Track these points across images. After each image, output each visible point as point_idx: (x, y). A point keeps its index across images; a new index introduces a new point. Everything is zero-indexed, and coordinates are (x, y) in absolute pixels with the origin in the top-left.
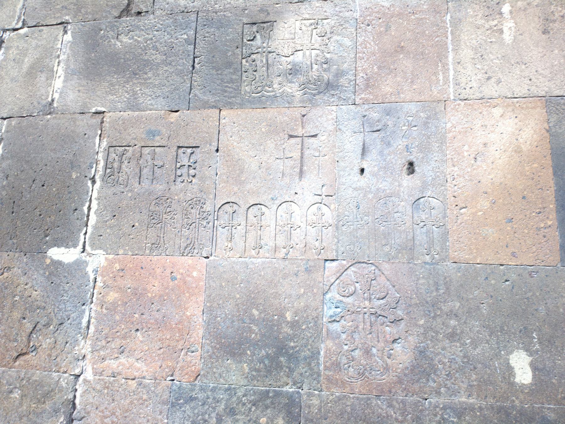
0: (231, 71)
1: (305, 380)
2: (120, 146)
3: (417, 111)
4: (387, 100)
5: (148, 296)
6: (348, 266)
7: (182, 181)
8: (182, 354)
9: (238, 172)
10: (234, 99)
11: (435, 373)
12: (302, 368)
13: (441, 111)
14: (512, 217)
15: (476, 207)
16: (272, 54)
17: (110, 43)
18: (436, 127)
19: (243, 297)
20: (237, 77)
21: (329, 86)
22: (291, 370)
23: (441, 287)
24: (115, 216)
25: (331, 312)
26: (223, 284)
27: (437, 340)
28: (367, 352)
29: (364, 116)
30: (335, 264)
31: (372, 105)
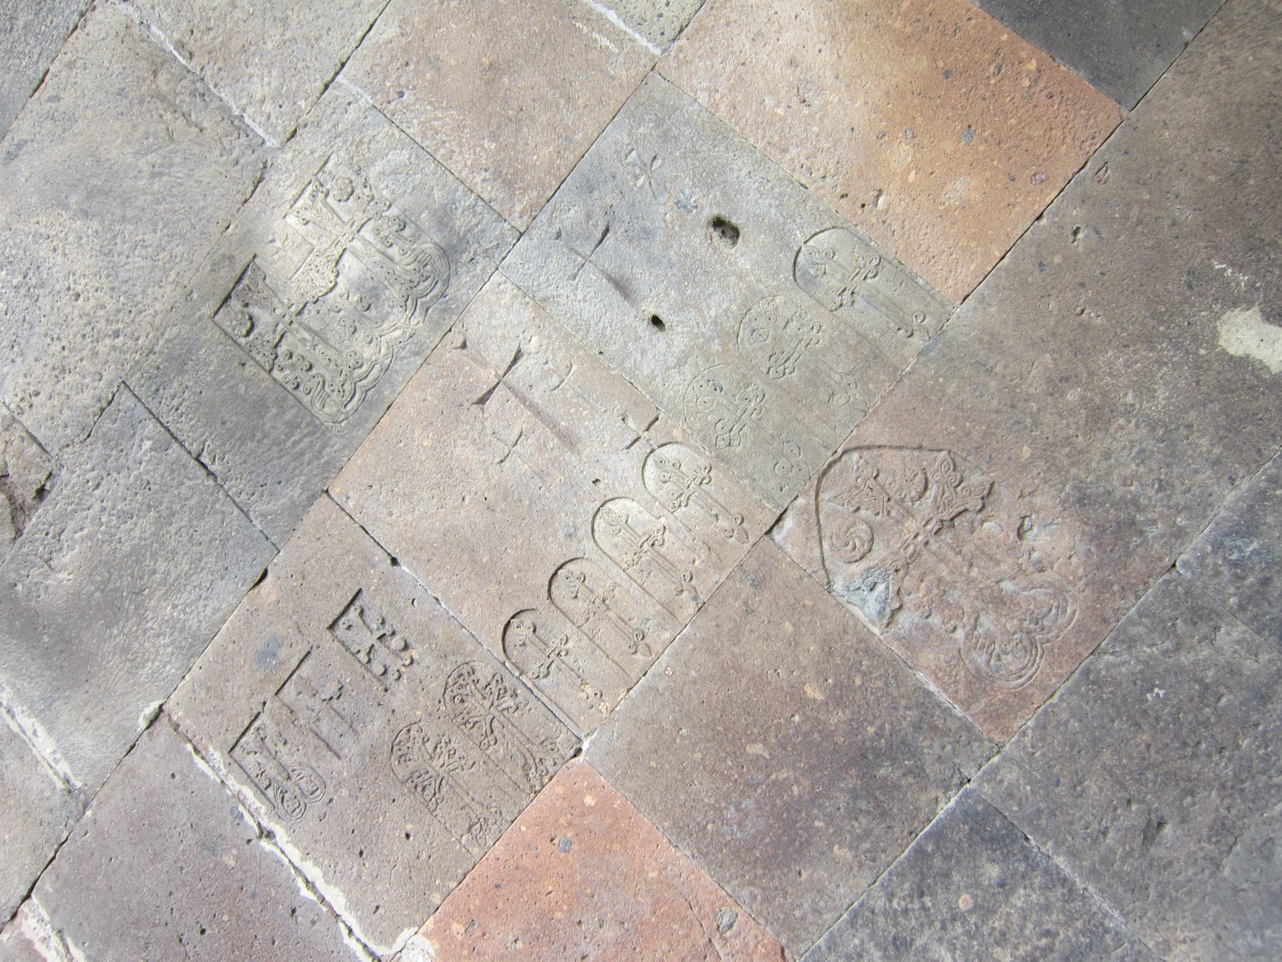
0: (274, 411)
1: (957, 761)
2: (243, 734)
3: (630, 134)
4: (563, 170)
5: (559, 921)
6: (812, 501)
7: (396, 676)
8: (718, 947)
9: (465, 558)
10: (328, 450)
11: (1139, 509)
12: (929, 748)
13: (665, 91)
14: (966, 124)
15: (894, 174)
16: (306, 311)
17: (51, 589)
18: (687, 123)
19: (706, 748)
20: (294, 411)
21: (450, 253)
22: (918, 772)
23: (992, 362)
24: (361, 853)
25: (873, 606)
26: (653, 764)
27: (1081, 452)
28: (999, 601)
29: (559, 236)
30: (788, 522)
31: (550, 206)
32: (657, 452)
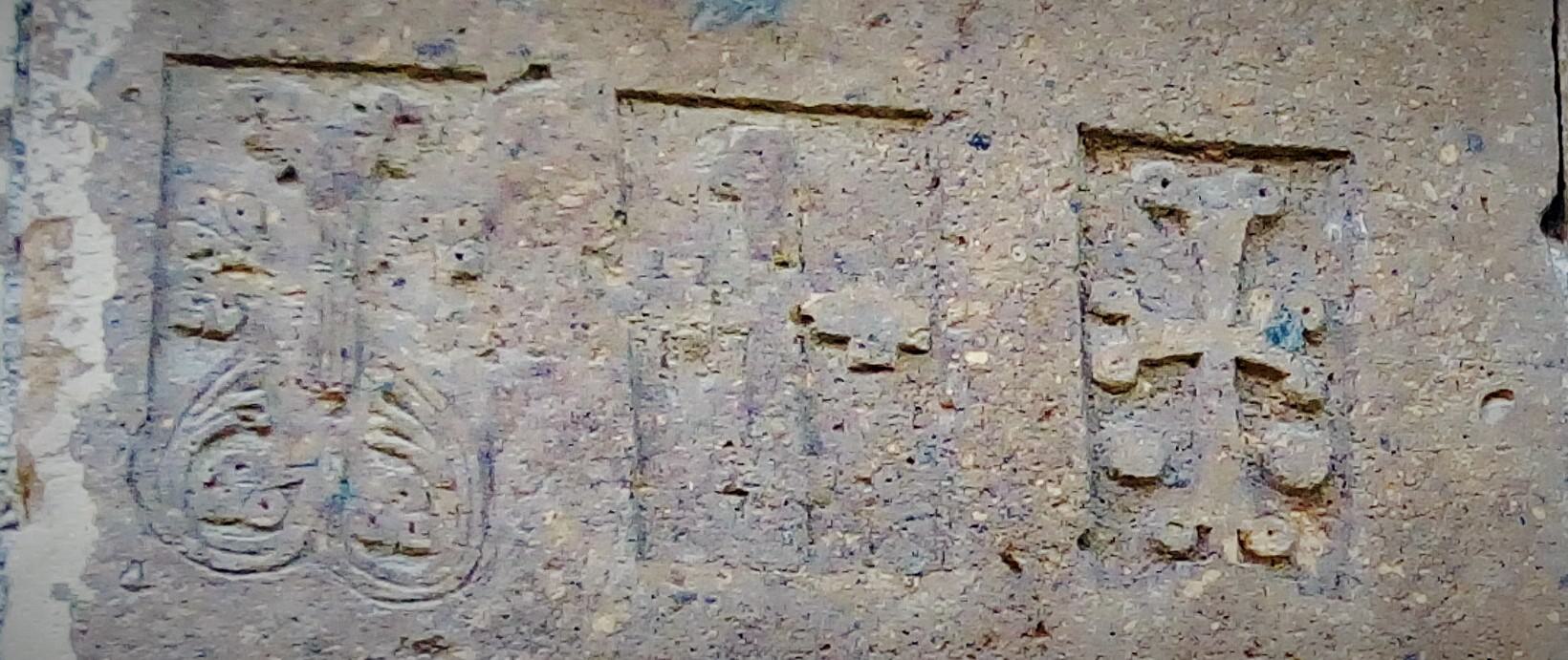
2: (317, 67)
7: (1179, 539)
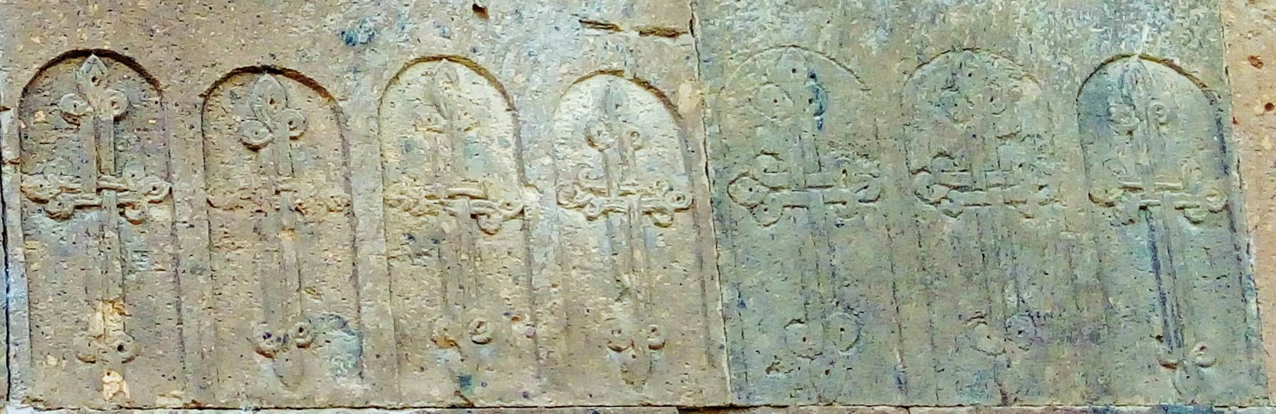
32: (622, 81)
